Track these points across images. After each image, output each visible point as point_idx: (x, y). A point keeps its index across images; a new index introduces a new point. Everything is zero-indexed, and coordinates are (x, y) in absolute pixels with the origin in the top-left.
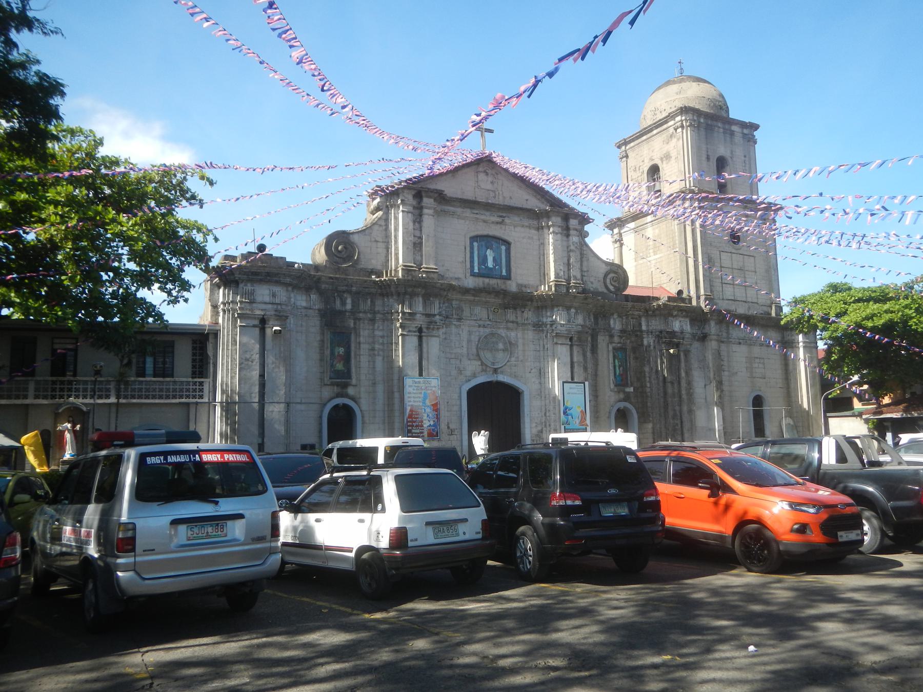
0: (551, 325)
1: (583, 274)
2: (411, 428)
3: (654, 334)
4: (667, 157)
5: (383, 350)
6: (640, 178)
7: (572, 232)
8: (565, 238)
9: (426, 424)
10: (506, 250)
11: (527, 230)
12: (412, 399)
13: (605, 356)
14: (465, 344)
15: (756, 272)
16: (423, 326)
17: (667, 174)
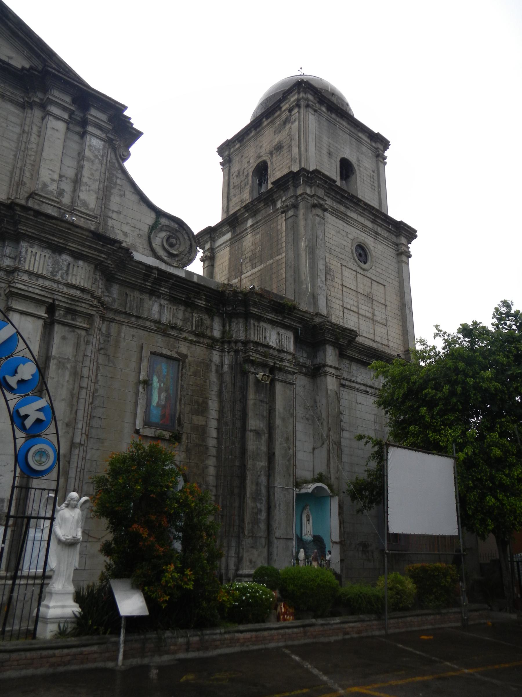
1: (110, 214)
3: (233, 345)
4: (279, 147)
6: (243, 183)
7: (90, 129)
8: (76, 138)
13: (133, 365)
15: (386, 306)
17: (277, 169)
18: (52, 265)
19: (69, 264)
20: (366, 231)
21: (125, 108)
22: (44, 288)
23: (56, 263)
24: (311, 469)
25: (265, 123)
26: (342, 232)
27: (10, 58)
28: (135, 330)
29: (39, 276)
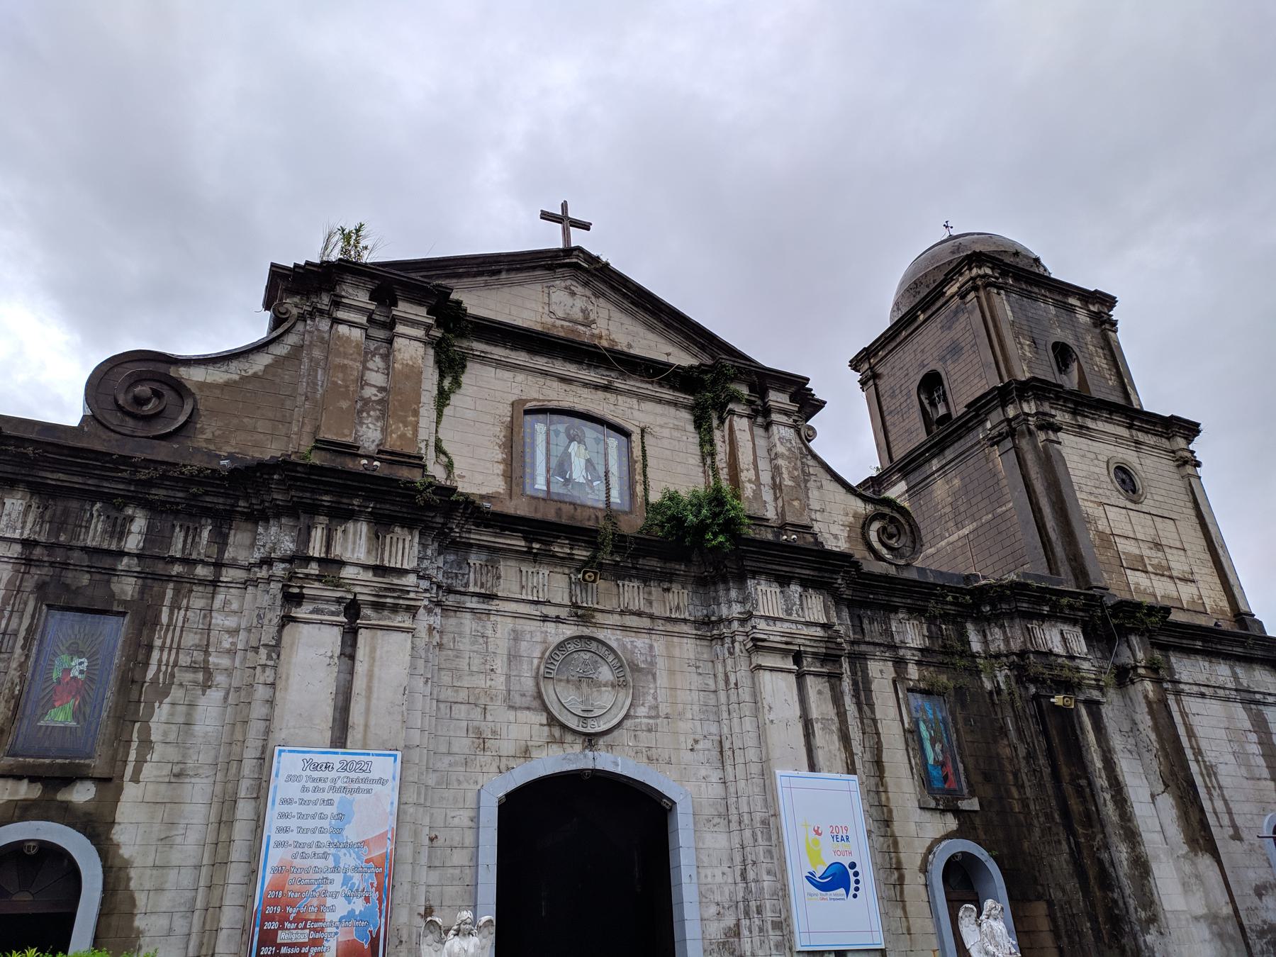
0: (743, 622)
2: (275, 925)
4: (955, 350)
5: (229, 672)
7: (775, 417)
8: (759, 432)
9: (338, 908)
10: (619, 447)
11: (672, 410)
12: (293, 823)
14: (500, 664)
15: (1184, 550)
16: (359, 597)
18: (785, 601)
19: (801, 596)
20: (1122, 444)
21: (808, 380)
22: (783, 634)
23: (787, 599)
24: (1159, 829)
25: (922, 317)
26: (1089, 455)
27: (668, 354)
28: (881, 663)
29: (775, 619)
